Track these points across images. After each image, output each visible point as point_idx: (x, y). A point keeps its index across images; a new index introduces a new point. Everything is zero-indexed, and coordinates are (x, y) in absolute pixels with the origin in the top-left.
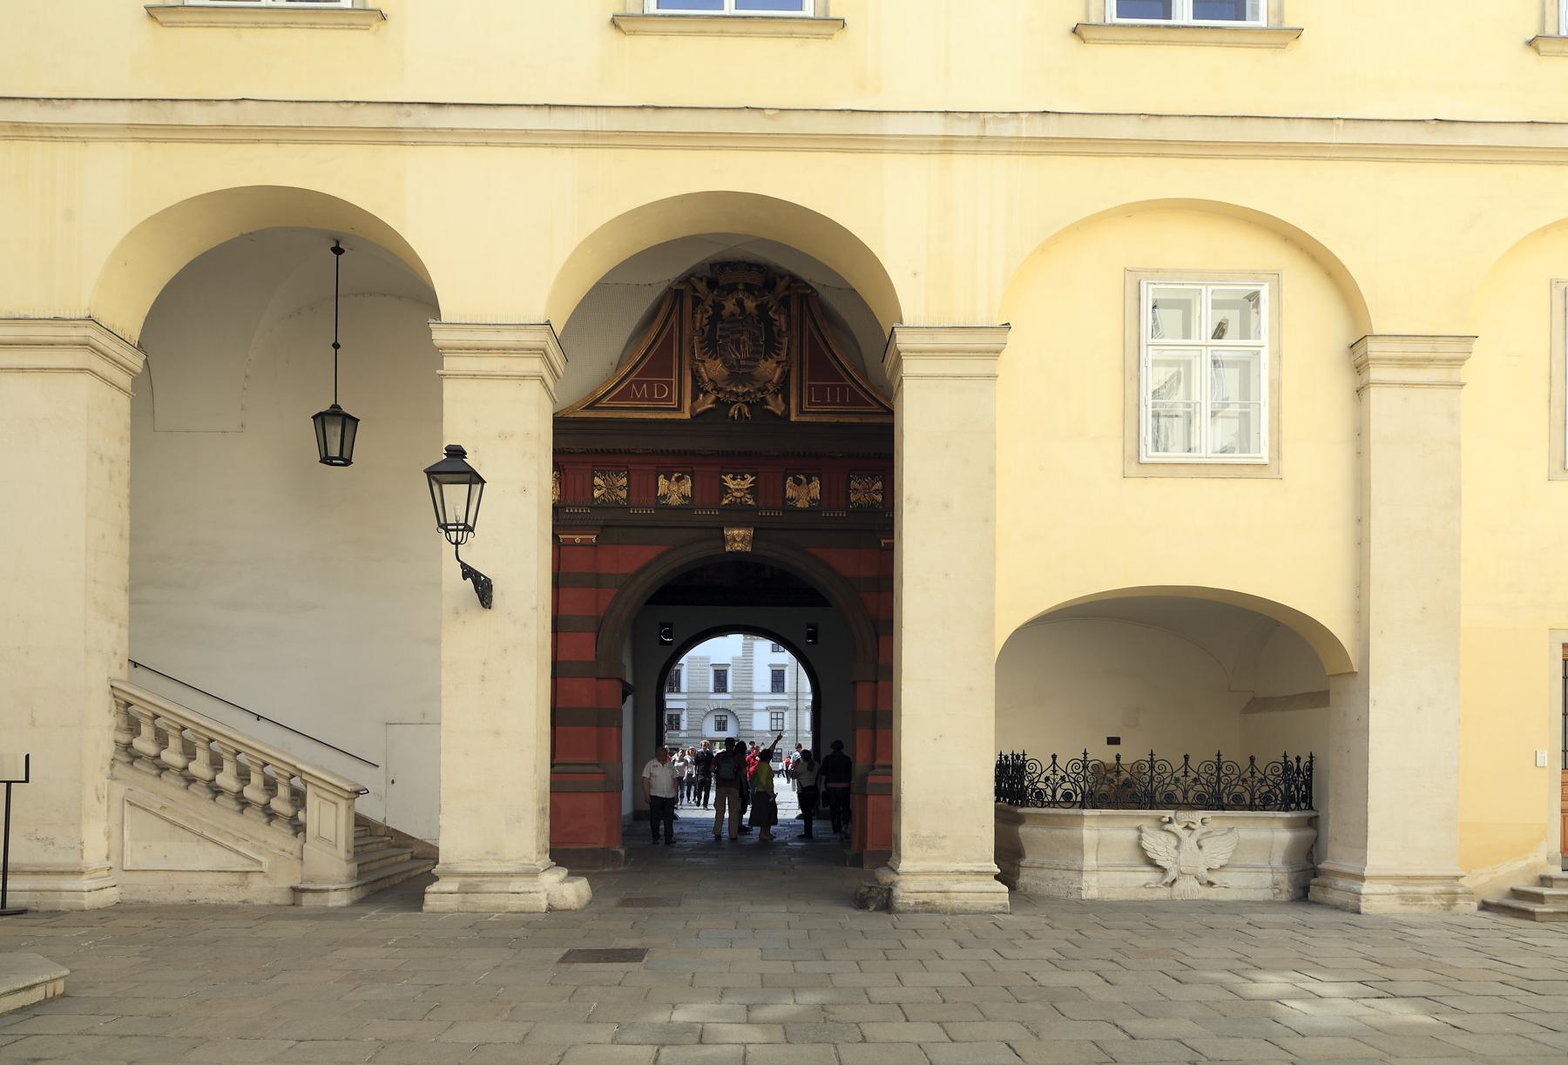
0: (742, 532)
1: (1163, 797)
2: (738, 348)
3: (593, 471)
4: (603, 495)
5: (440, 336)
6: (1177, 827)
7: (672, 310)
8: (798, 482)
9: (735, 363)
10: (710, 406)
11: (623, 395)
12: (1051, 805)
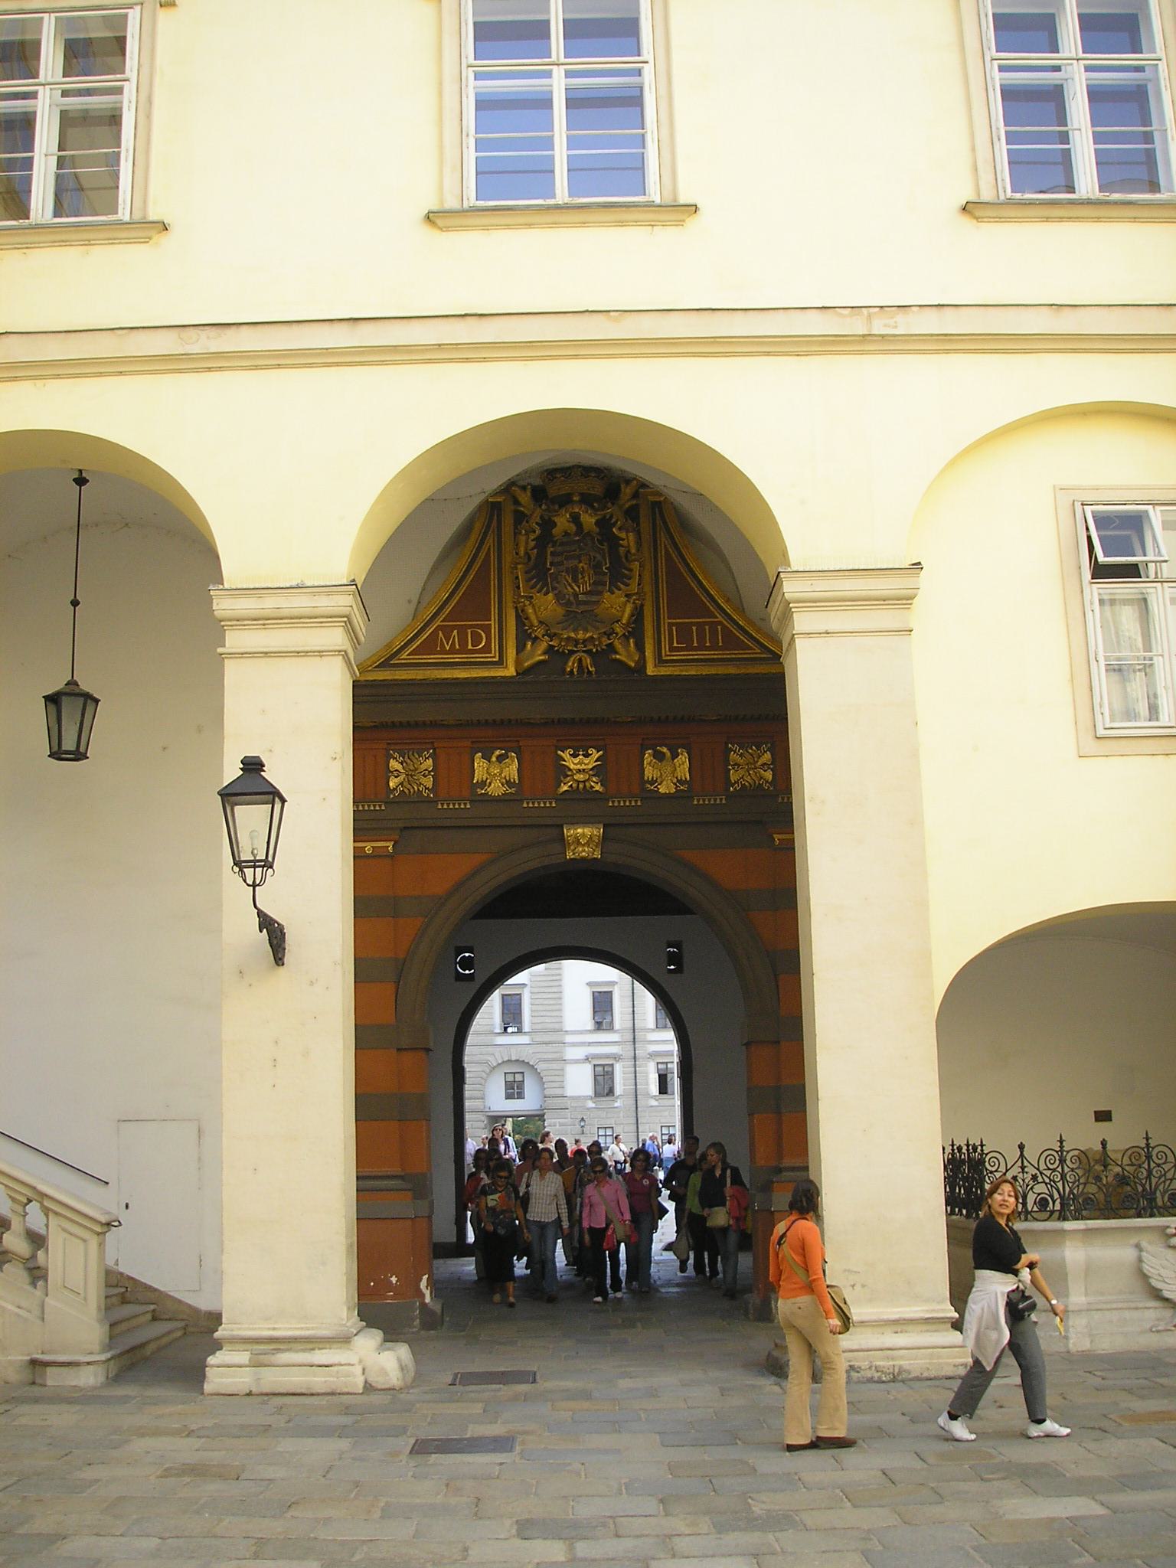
0: (588, 831)
1: (1166, 1199)
2: (575, 580)
3: (387, 750)
4: (402, 784)
5: (222, 605)
7: (486, 534)
8: (659, 757)
9: (572, 598)
10: (541, 658)
11: (429, 647)
12: (1022, 1217)
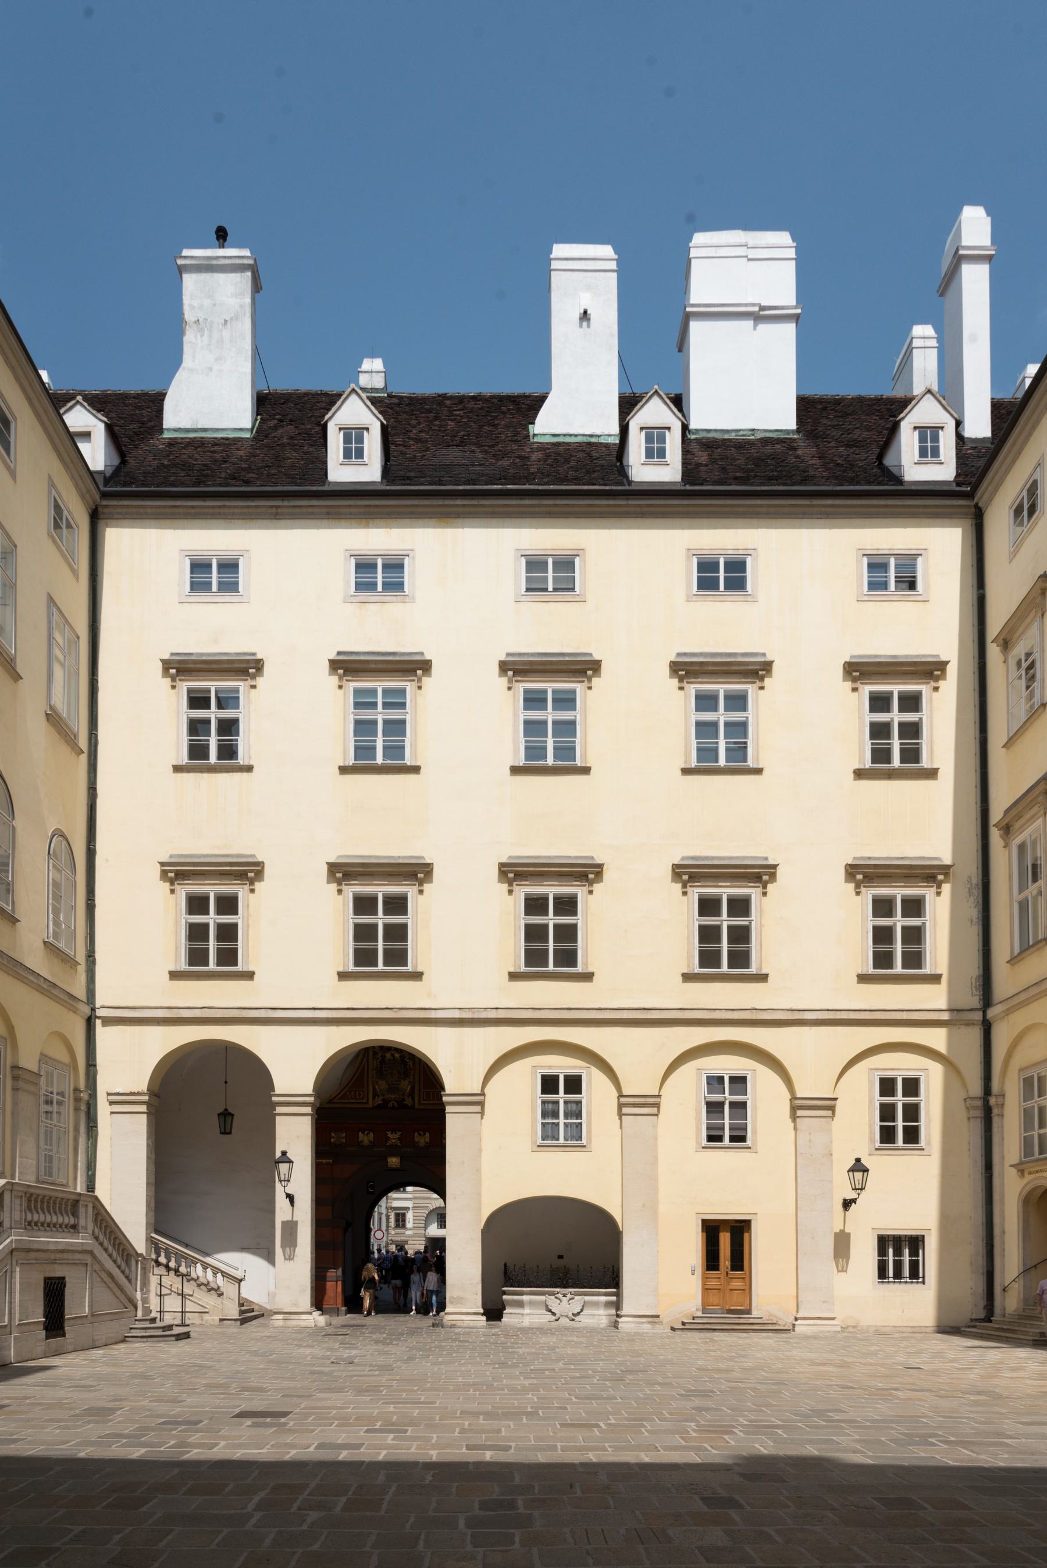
6: (560, 1296)
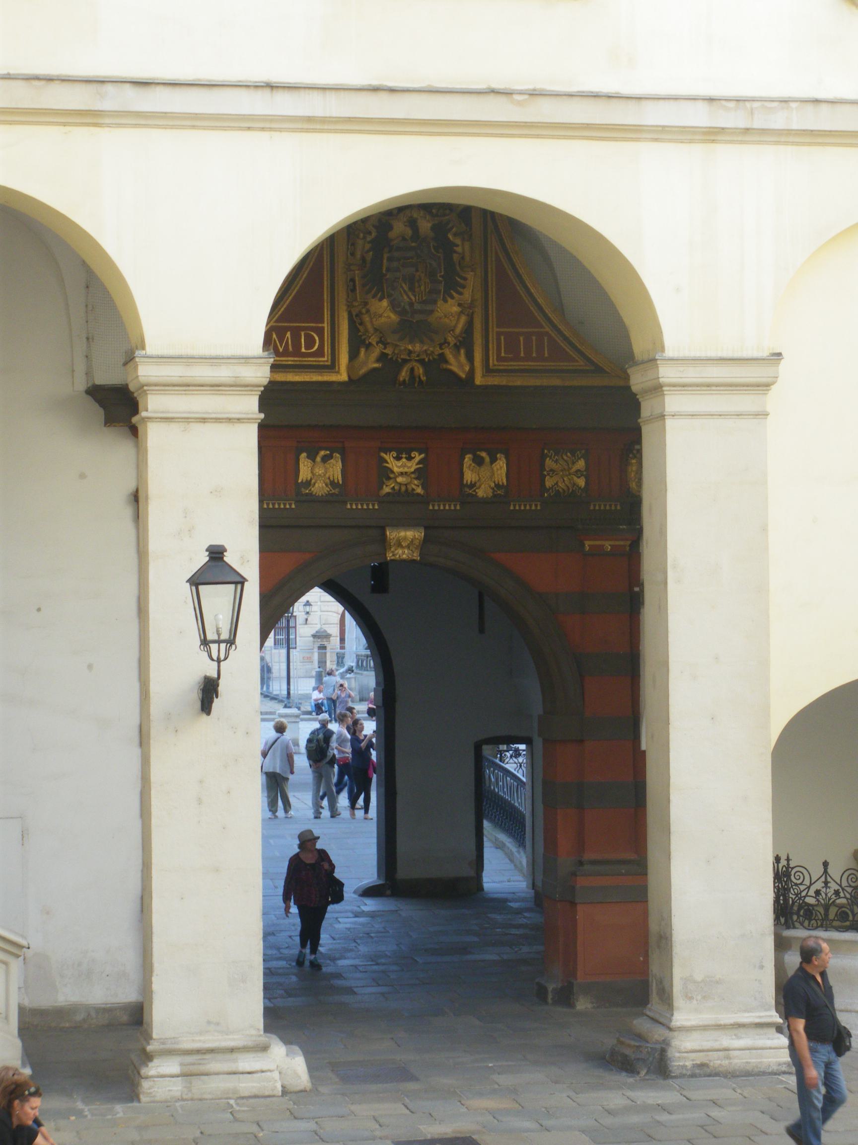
2: (412, 289)
8: (479, 461)
9: (407, 307)
